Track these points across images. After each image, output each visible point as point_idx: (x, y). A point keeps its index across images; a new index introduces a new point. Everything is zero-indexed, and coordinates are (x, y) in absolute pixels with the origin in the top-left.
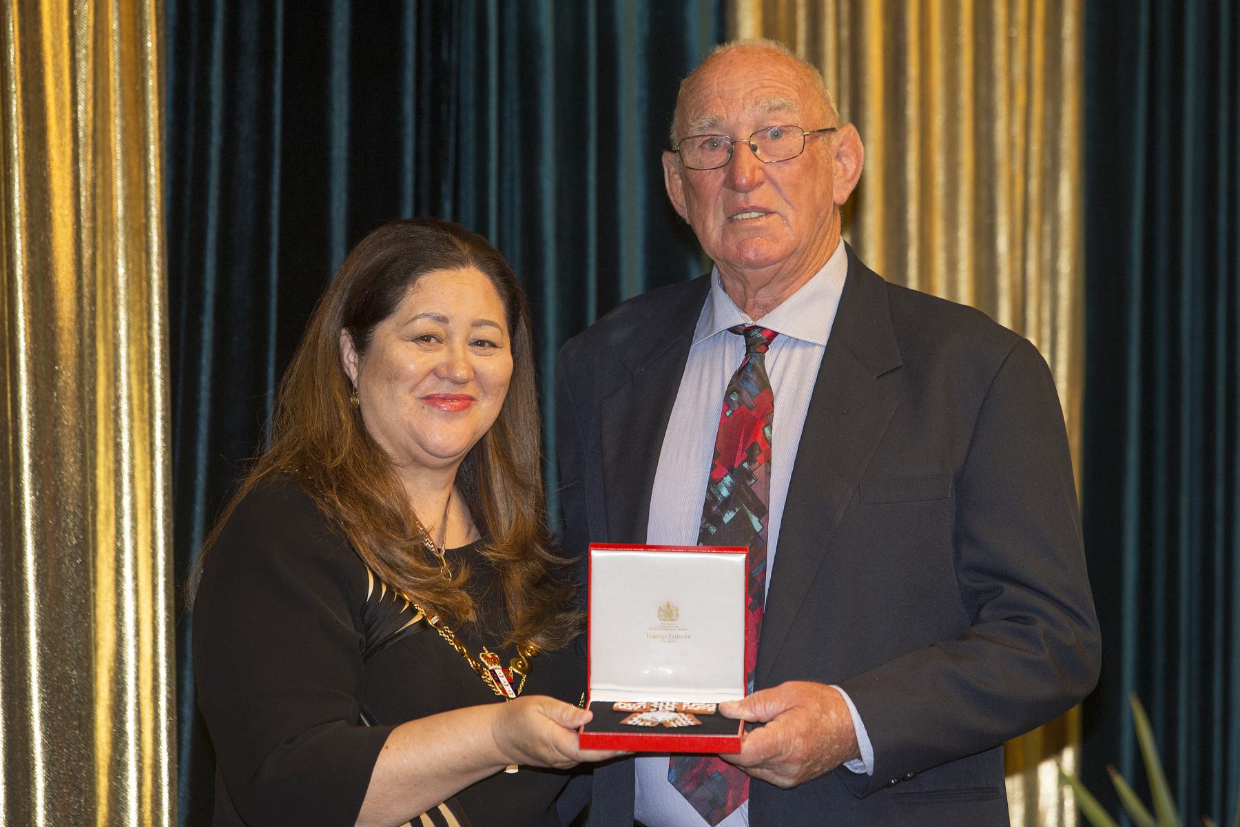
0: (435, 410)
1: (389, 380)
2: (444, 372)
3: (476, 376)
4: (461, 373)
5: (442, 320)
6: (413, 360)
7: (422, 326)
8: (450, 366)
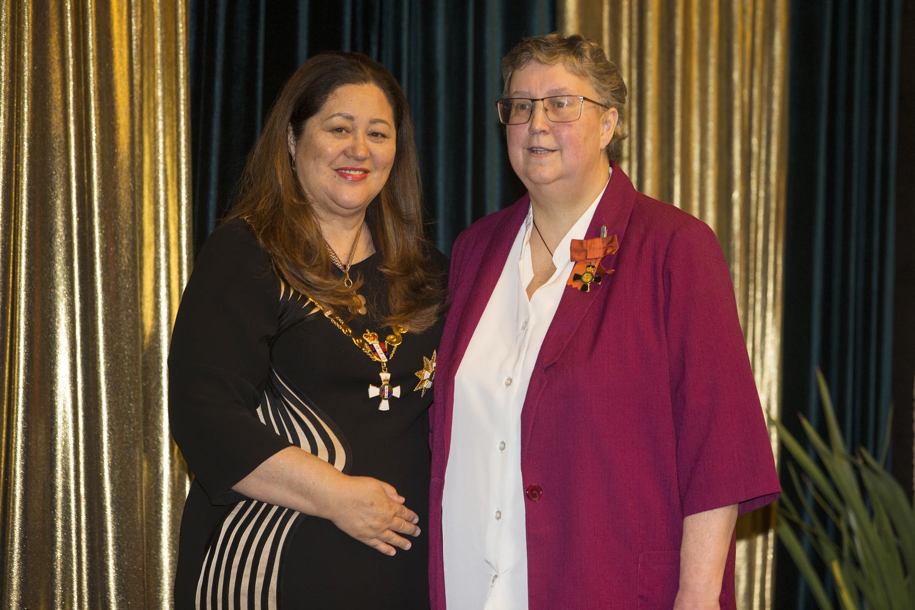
0: (343, 179)
1: (315, 158)
2: (350, 153)
3: (371, 156)
4: (361, 153)
5: (351, 118)
6: (331, 145)
7: (337, 121)
8: (354, 148)
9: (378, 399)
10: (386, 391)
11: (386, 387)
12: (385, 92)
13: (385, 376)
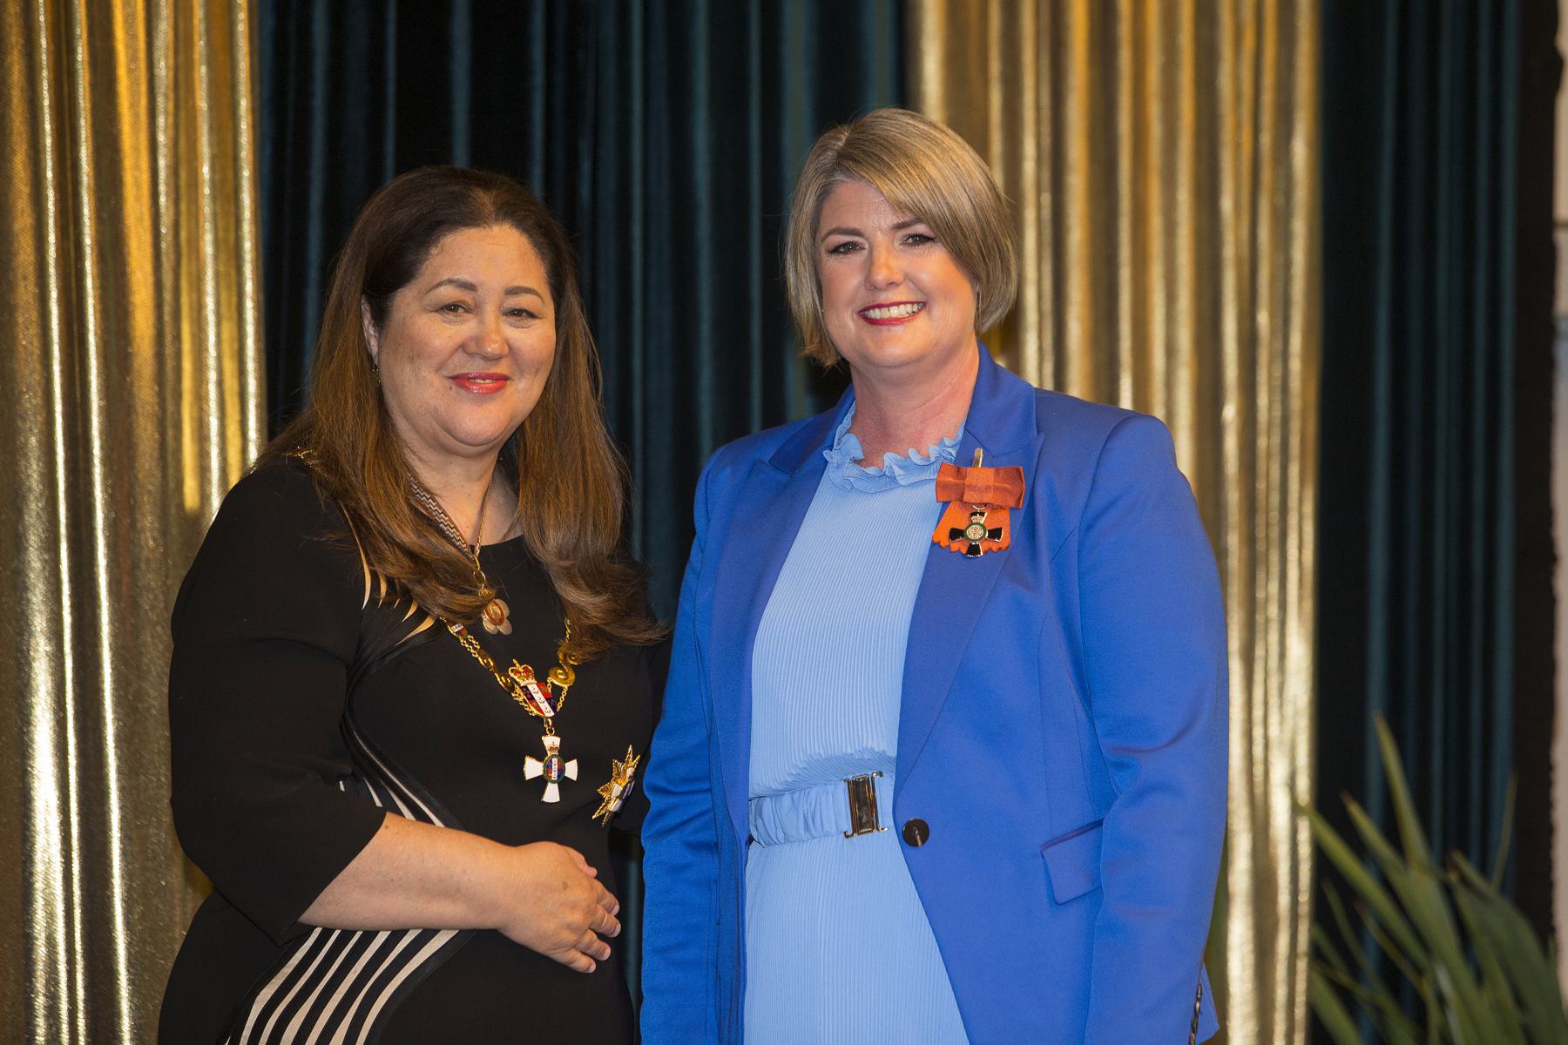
0: (463, 392)
1: (412, 359)
2: (472, 347)
3: (512, 351)
4: (492, 348)
5: (470, 287)
6: (442, 334)
7: (448, 293)
8: (479, 340)
9: (541, 782)
10: (555, 767)
11: (555, 760)
13: (551, 741)
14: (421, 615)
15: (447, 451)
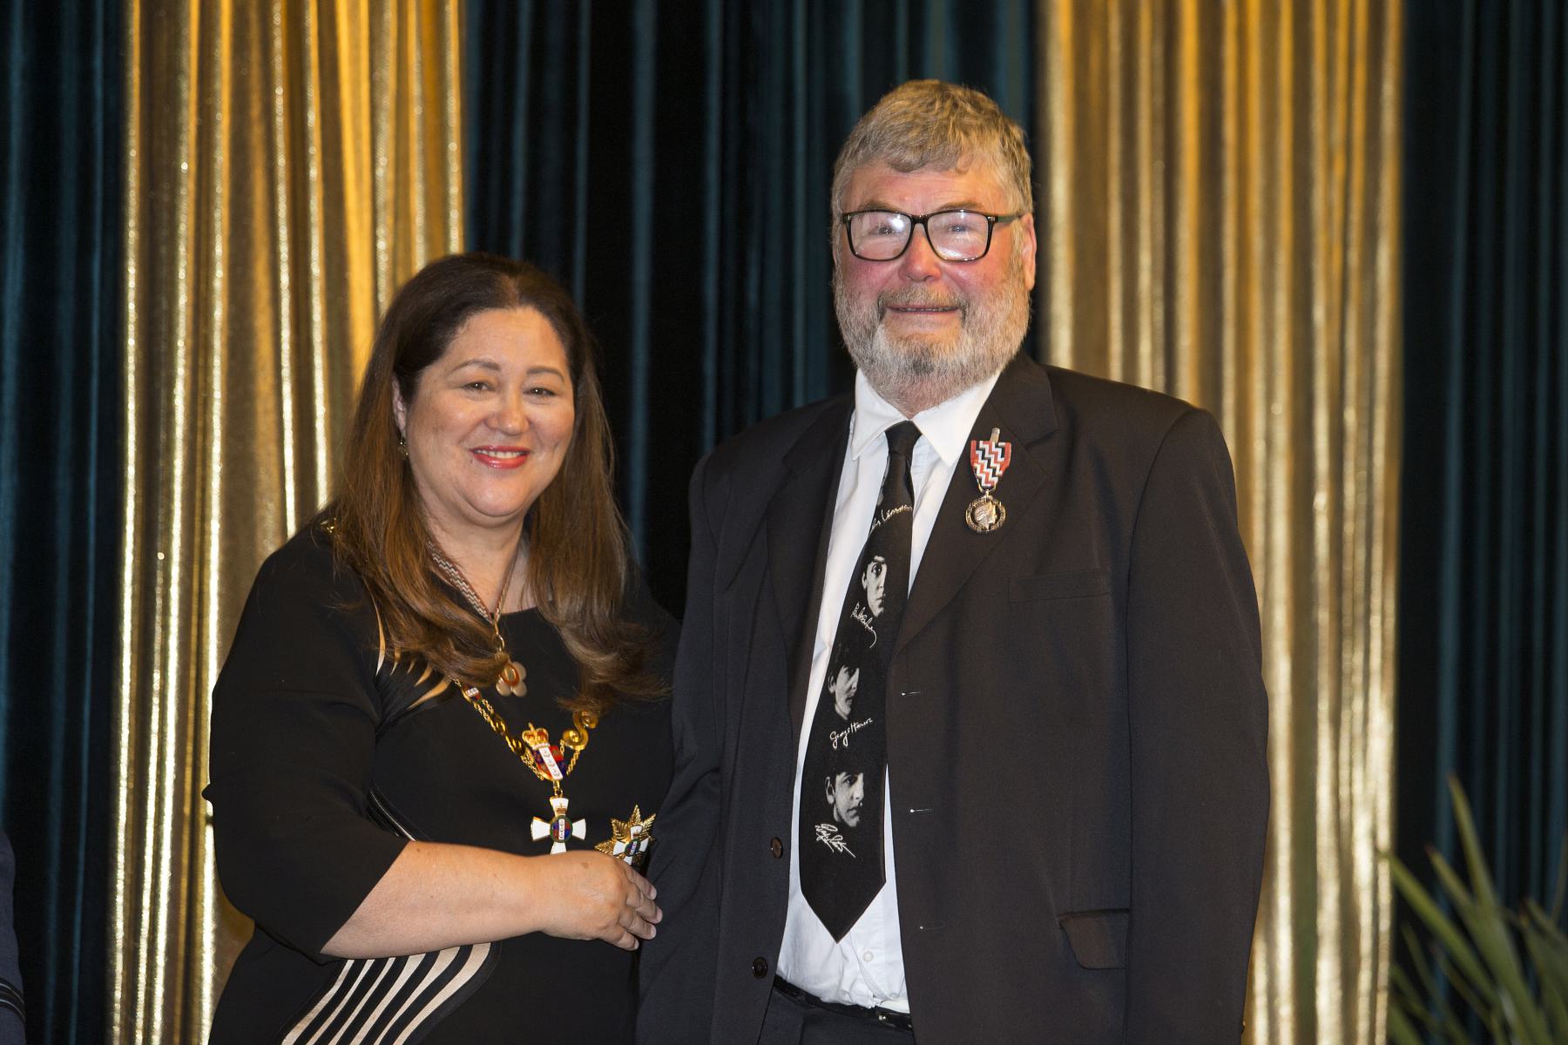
1: (436, 431)
2: (494, 423)
4: (513, 424)
5: (493, 367)
6: (464, 409)
7: (472, 373)
8: (501, 416)
10: (562, 828)
11: (562, 822)
12: (552, 319)
13: (559, 803)
14: (436, 678)
15: (469, 521)
